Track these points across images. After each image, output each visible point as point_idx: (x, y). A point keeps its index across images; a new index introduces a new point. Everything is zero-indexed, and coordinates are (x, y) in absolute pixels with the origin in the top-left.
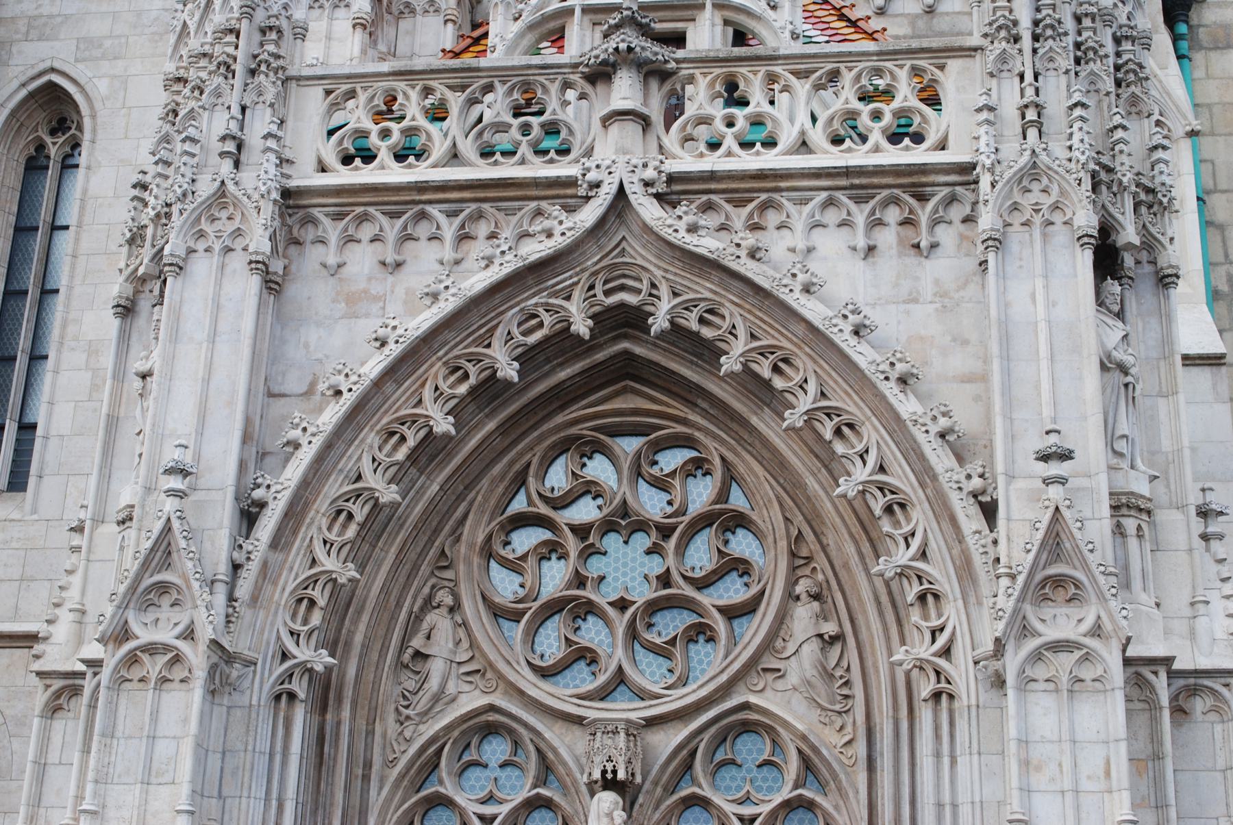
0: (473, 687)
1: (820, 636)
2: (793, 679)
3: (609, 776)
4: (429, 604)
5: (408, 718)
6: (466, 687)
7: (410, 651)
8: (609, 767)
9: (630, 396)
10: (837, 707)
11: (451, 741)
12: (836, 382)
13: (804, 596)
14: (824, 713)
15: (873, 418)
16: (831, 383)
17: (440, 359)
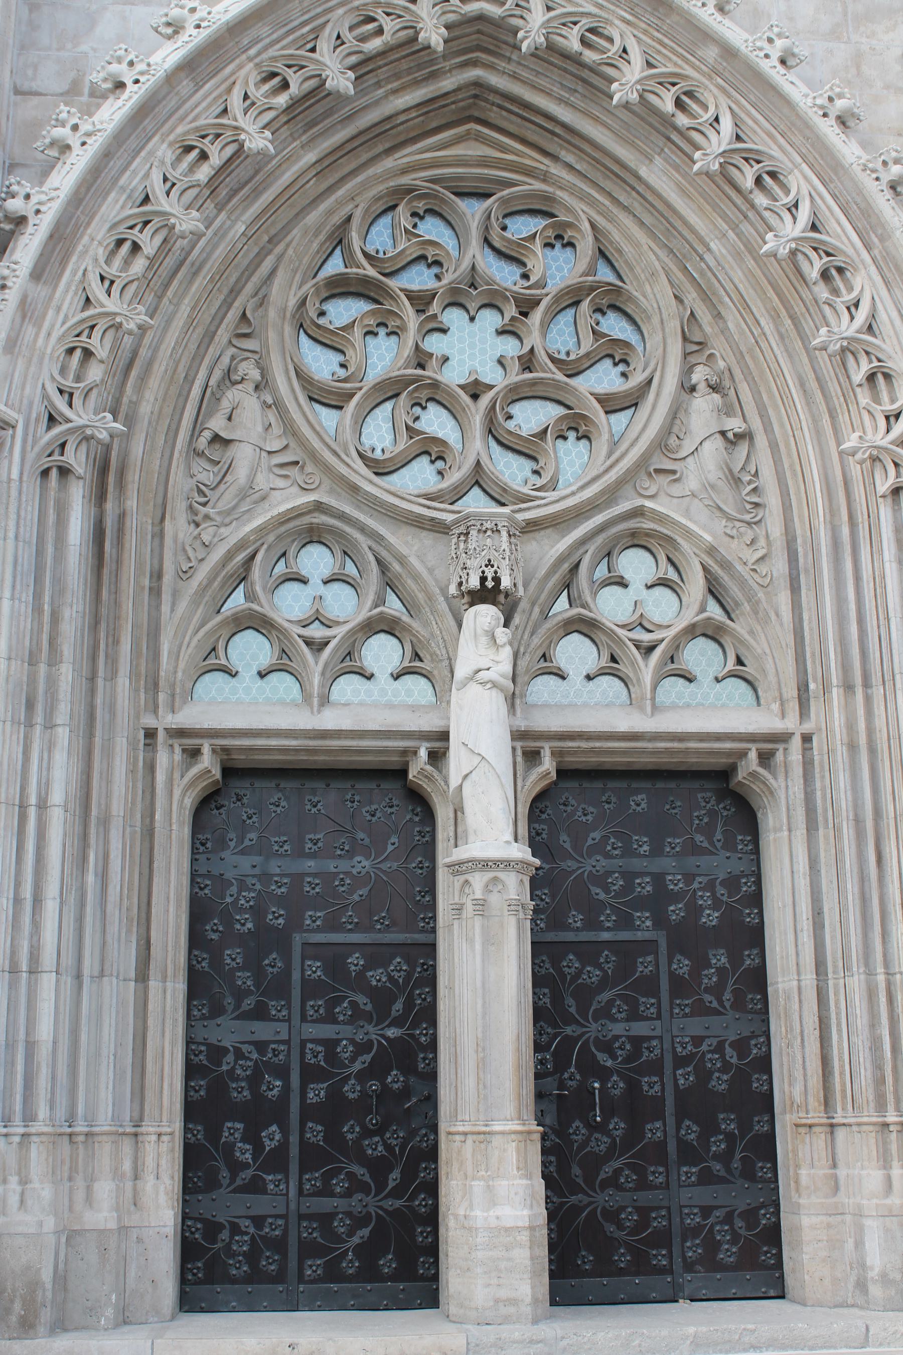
0: (289, 482)
1: (723, 433)
2: (692, 483)
3: (490, 584)
4: (230, 379)
5: (207, 517)
6: (281, 483)
7: (207, 434)
8: (489, 574)
9: (473, 144)
10: (747, 517)
11: (265, 546)
12: (756, 121)
13: (702, 387)
14: (730, 525)
15: (804, 166)
16: (750, 122)
17: (250, 59)
